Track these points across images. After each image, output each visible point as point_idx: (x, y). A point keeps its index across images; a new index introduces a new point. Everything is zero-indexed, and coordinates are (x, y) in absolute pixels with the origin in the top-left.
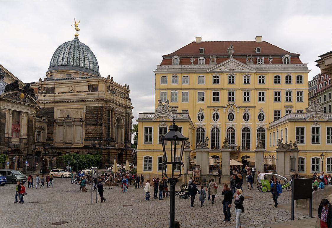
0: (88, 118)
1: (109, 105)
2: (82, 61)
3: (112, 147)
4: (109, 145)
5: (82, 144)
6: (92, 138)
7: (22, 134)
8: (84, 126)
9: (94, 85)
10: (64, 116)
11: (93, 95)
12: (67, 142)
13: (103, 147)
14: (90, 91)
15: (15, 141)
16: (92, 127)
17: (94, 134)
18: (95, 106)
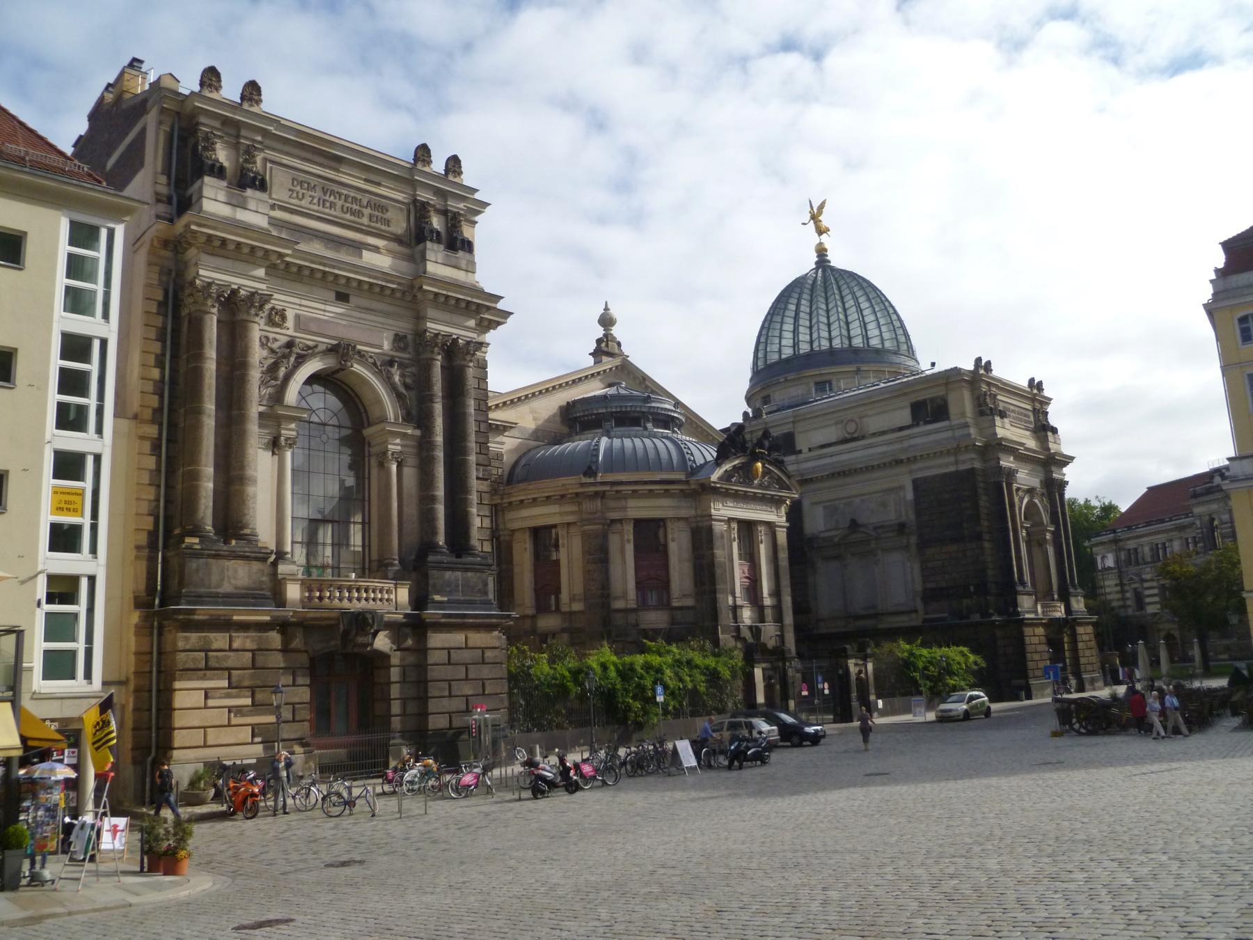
1: (993, 463)
2: (856, 330)
5: (914, 615)
9: (932, 400)
18: (945, 475)
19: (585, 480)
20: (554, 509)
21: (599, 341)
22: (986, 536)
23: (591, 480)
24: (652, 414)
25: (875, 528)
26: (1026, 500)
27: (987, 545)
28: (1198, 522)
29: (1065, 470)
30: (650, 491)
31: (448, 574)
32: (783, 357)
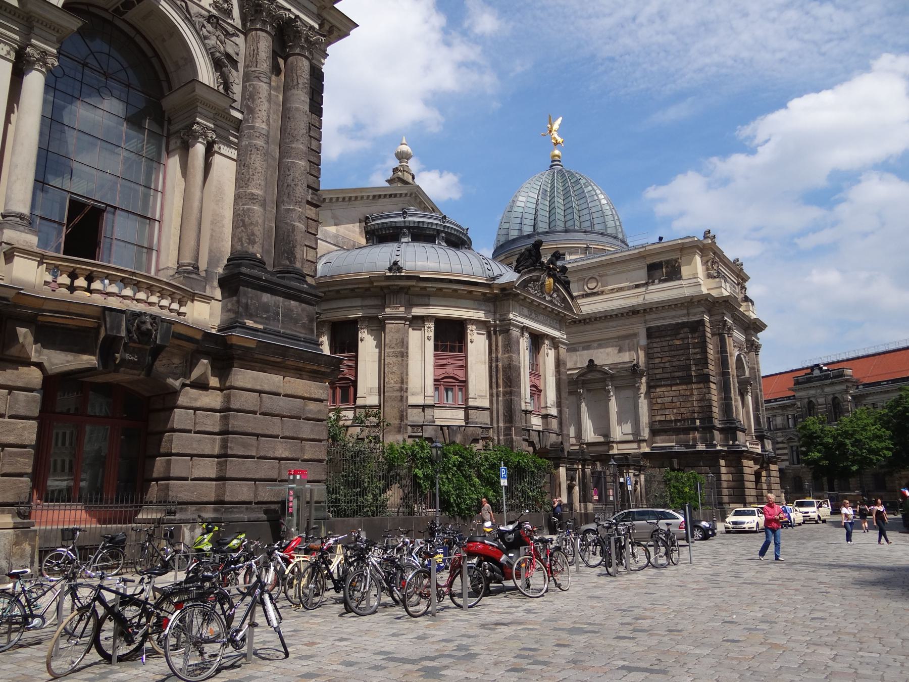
0: (657, 361)
4: (737, 443)
6: (676, 421)
9: (667, 262)
10: (576, 363)
11: (661, 292)
13: (719, 448)
14: (657, 281)
16: (673, 388)
17: (682, 410)
18: (677, 324)
21: (395, 170)
22: (712, 379)
24: (446, 233)
26: (737, 353)
27: (713, 386)
28: (799, 403)
29: (759, 335)
30: (456, 290)
31: (266, 297)
32: (525, 233)
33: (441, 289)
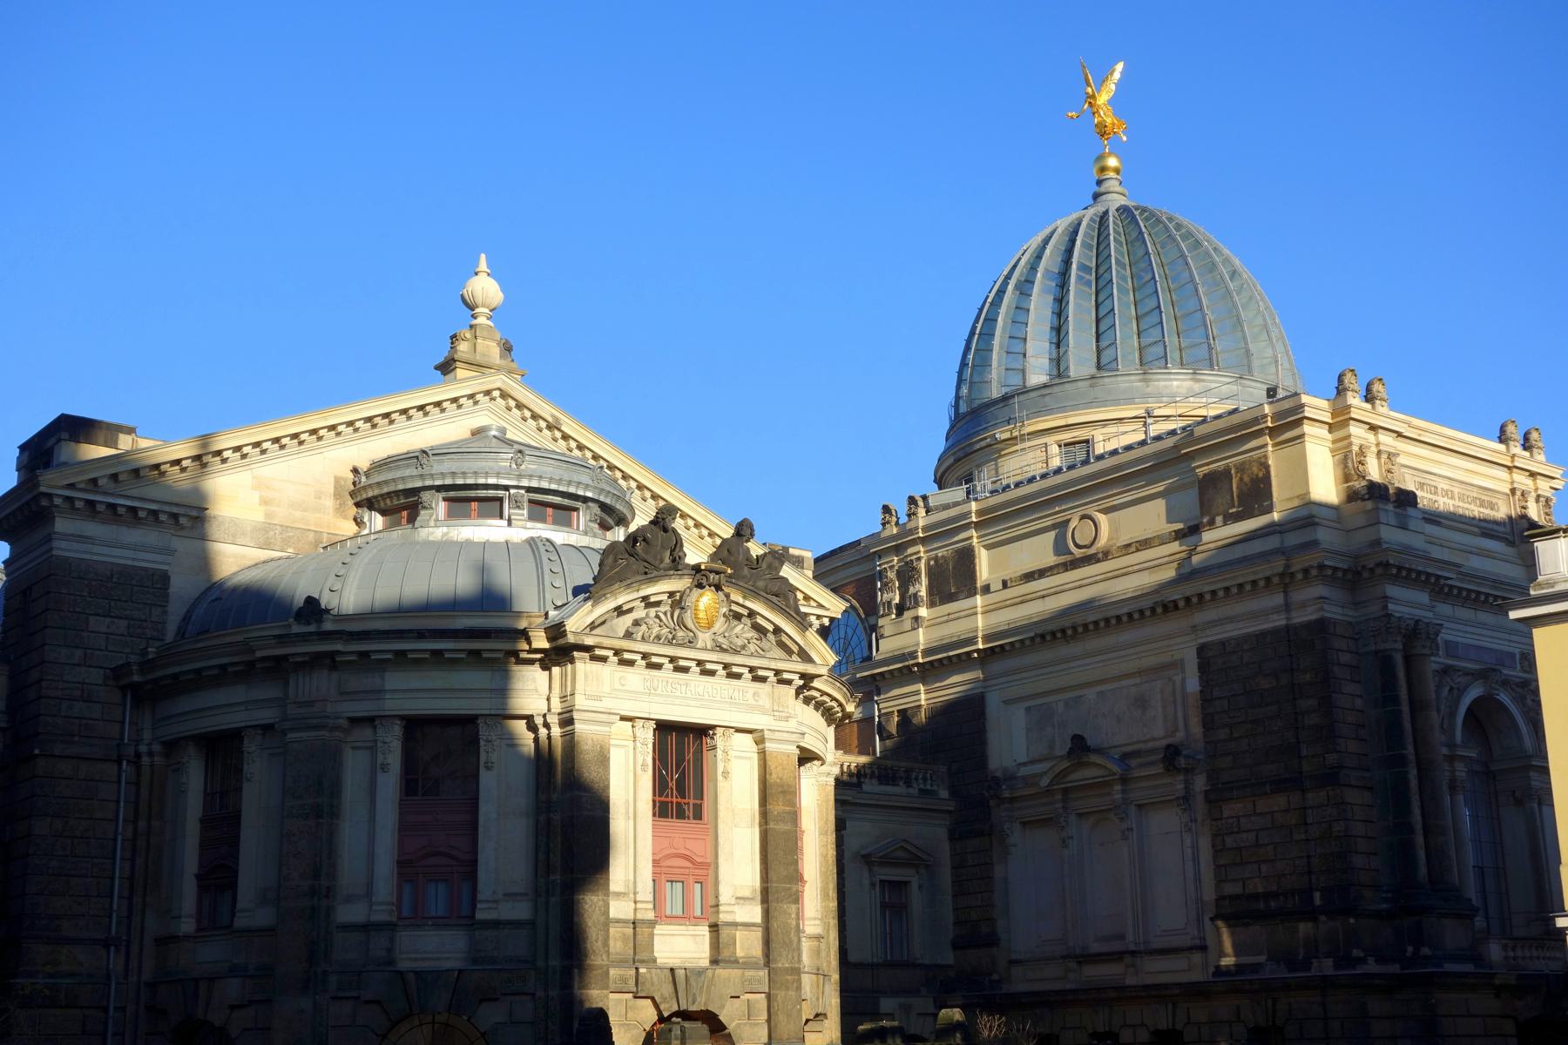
0: (1222, 734)
3: (1449, 967)
4: (1426, 951)
5: (1197, 957)
6: (1267, 896)
7: (726, 895)
8: (1199, 804)
9: (1241, 468)
12: (1096, 947)
13: (1372, 967)
14: (1219, 520)
15: (679, 946)
18: (1263, 635)
19: (296, 629)
20: (238, 693)
23: (312, 628)
25: (1125, 756)
26: (1475, 692)
30: (437, 653)
33: (401, 654)
